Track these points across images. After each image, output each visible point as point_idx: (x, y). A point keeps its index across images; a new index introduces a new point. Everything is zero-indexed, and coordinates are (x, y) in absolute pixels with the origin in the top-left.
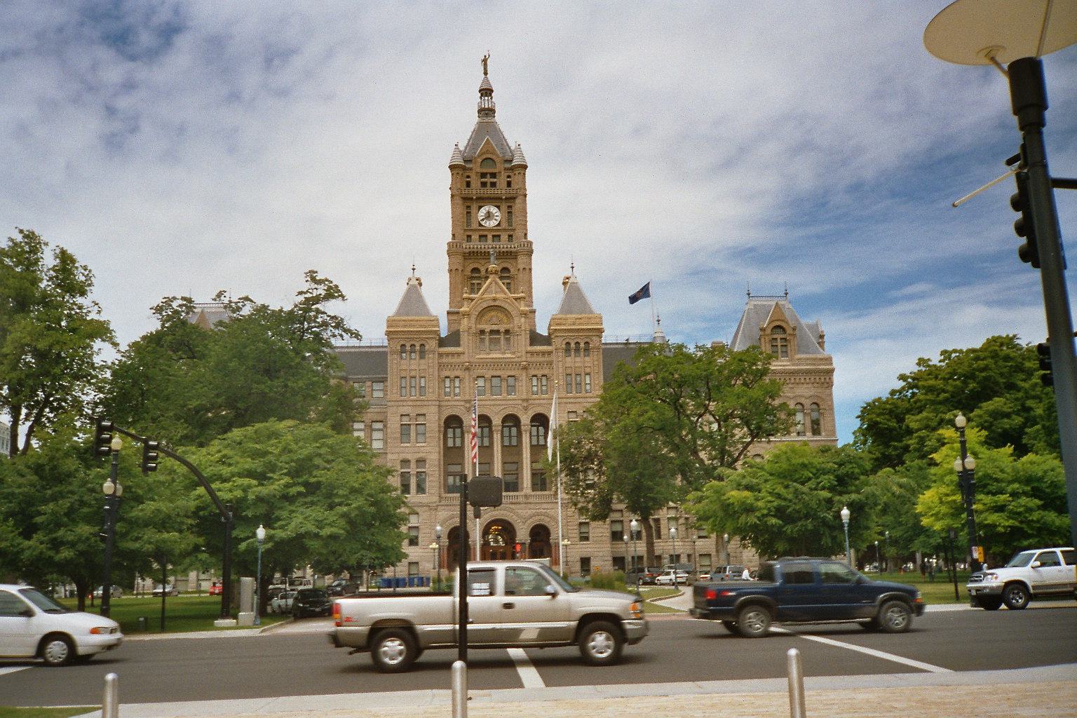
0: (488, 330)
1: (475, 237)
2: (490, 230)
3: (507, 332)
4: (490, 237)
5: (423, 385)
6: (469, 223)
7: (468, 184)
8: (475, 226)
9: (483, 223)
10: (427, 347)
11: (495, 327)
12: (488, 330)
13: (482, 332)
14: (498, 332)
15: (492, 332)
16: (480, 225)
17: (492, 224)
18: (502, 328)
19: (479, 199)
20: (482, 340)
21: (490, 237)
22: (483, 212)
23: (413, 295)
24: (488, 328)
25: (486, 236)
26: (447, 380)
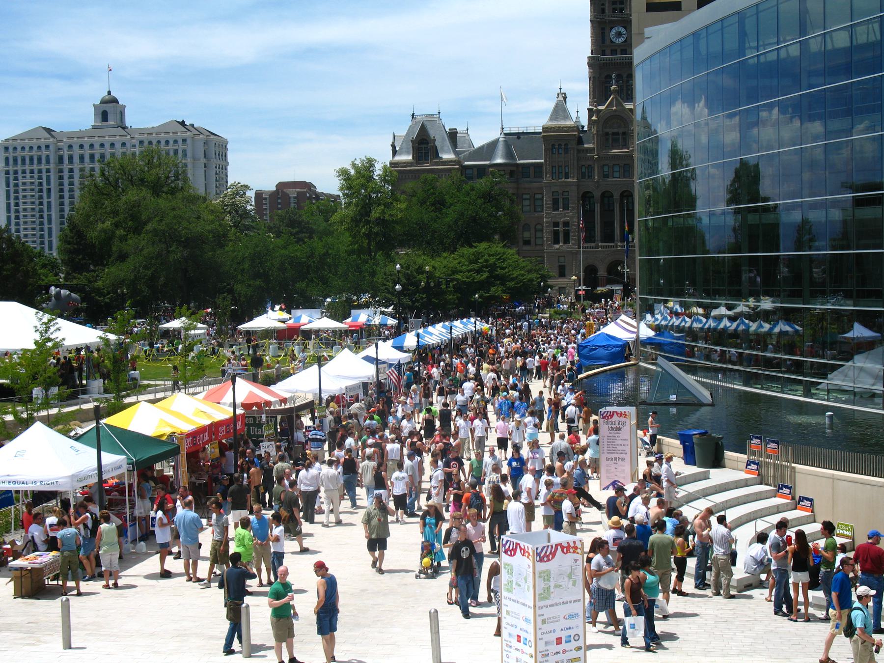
0: (610, 132)
1: (608, 51)
2: (619, 45)
3: (624, 133)
4: (619, 51)
5: (567, 171)
6: (603, 41)
7: (603, 11)
8: (608, 42)
9: (614, 40)
10: (569, 146)
11: (615, 130)
12: (610, 132)
13: (607, 134)
14: (617, 134)
15: (614, 134)
16: (612, 42)
17: (621, 40)
18: (621, 131)
19: (610, 22)
20: (607, 140)
21: (619, 51)
22: (613, 32)
23: (560, 110)
24: (610, 131)
25: (616, 50)
26: (584, 168)
